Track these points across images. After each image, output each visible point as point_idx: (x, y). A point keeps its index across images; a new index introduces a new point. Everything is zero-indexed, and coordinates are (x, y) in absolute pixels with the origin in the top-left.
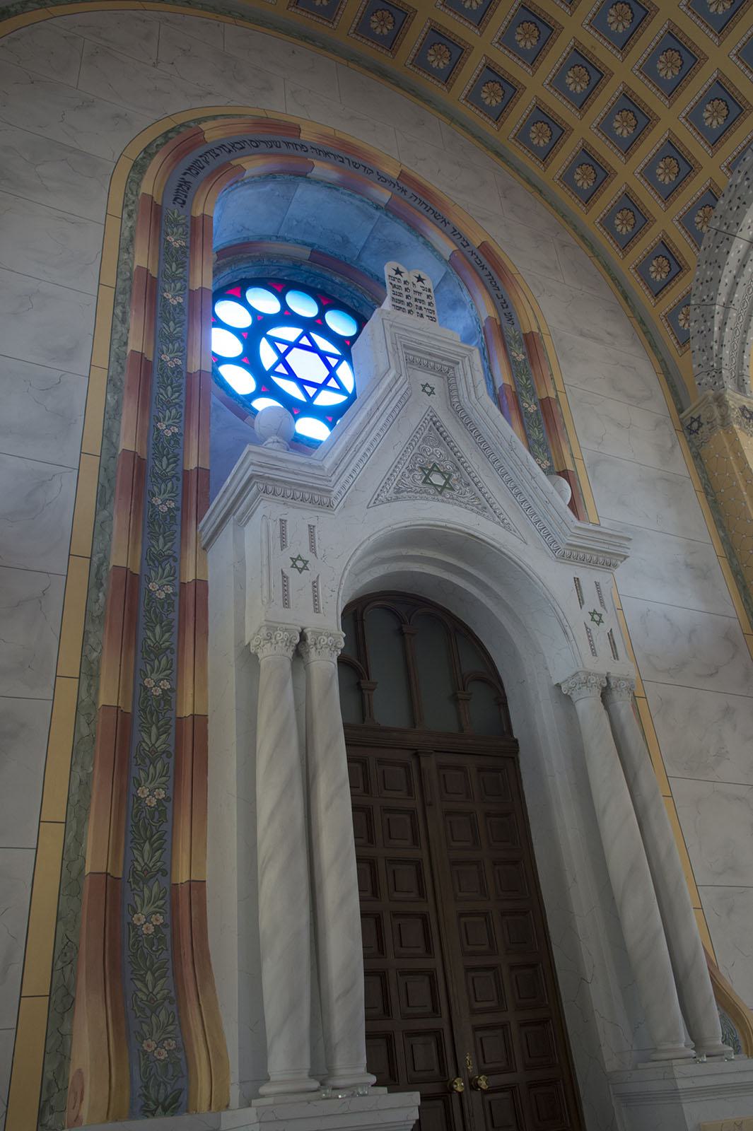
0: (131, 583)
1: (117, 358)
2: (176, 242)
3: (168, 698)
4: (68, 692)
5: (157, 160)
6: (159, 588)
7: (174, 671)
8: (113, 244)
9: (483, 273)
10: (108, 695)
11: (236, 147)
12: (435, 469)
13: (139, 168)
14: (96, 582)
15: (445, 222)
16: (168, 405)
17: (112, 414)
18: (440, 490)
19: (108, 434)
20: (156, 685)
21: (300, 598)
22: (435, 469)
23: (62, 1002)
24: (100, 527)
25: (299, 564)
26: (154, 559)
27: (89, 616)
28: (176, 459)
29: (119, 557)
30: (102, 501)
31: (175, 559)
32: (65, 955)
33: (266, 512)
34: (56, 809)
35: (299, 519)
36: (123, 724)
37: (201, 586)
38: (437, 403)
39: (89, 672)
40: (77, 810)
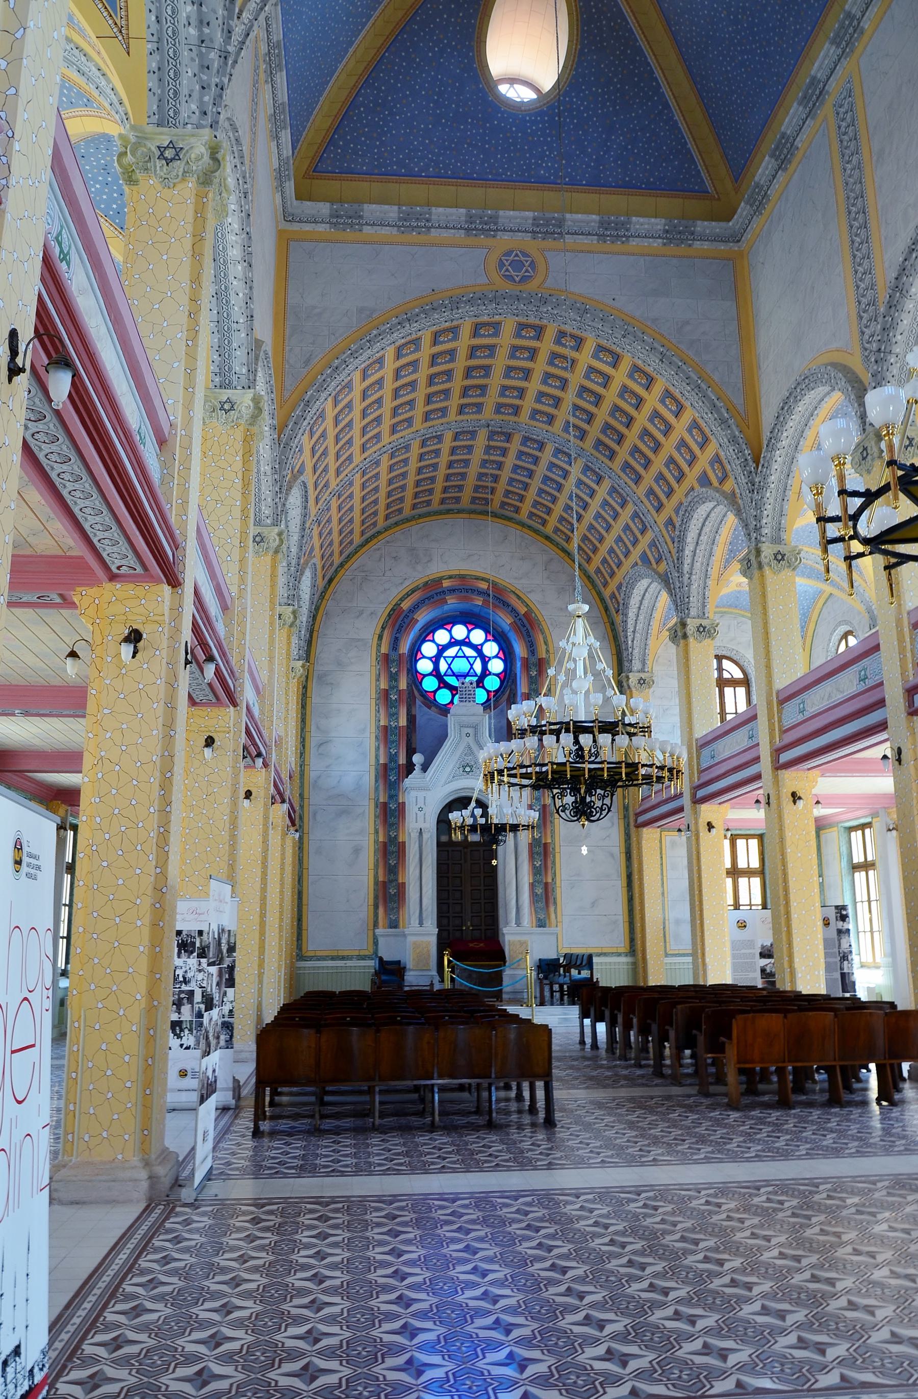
0: (385, 805)
1: (378, 727)
2: (393, 670)
3: (396, 837)
4: (372, 837)
5: (386, 632)
6: (393, 806)
7: (398, 832)
8: (374, 678)
9: (523, 629)
10: (381, 839)
11: (415, 608)
12: (468, 765)
13: (380, 637)
14: (376, 806)
15: (508, 605)
16: (393, 742)
17: (377, 749)
18: (468, 773)
19: (377, 757)
20: (393, 834)
21: (421, 819)
22: (468, 765)
23: (376, 907)
24: (376, 789)
25: (421, 809)
26: (391, 797)
27: (376, 816)
28: (396, 762)
29: (381, 800)
30: (376, 781)
31: (397, 795)
32: (376, 897)
33: (413, 794)
34: (372, 866)
35: (421, 794)
36: (385, 845)
37: (404, 803)
38: (470, 740)
39: (377, 832)
40: (376, 866)
